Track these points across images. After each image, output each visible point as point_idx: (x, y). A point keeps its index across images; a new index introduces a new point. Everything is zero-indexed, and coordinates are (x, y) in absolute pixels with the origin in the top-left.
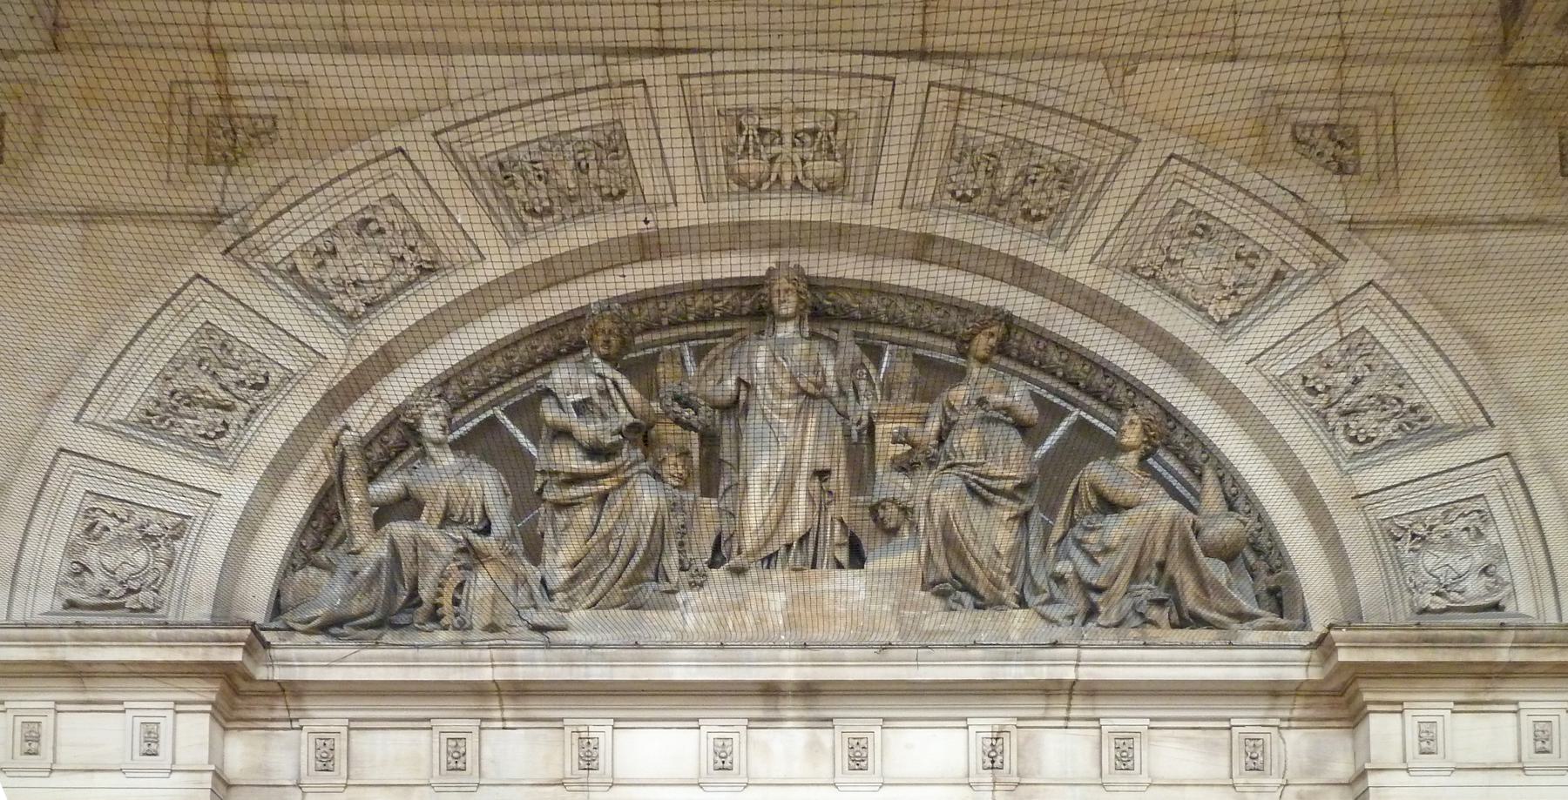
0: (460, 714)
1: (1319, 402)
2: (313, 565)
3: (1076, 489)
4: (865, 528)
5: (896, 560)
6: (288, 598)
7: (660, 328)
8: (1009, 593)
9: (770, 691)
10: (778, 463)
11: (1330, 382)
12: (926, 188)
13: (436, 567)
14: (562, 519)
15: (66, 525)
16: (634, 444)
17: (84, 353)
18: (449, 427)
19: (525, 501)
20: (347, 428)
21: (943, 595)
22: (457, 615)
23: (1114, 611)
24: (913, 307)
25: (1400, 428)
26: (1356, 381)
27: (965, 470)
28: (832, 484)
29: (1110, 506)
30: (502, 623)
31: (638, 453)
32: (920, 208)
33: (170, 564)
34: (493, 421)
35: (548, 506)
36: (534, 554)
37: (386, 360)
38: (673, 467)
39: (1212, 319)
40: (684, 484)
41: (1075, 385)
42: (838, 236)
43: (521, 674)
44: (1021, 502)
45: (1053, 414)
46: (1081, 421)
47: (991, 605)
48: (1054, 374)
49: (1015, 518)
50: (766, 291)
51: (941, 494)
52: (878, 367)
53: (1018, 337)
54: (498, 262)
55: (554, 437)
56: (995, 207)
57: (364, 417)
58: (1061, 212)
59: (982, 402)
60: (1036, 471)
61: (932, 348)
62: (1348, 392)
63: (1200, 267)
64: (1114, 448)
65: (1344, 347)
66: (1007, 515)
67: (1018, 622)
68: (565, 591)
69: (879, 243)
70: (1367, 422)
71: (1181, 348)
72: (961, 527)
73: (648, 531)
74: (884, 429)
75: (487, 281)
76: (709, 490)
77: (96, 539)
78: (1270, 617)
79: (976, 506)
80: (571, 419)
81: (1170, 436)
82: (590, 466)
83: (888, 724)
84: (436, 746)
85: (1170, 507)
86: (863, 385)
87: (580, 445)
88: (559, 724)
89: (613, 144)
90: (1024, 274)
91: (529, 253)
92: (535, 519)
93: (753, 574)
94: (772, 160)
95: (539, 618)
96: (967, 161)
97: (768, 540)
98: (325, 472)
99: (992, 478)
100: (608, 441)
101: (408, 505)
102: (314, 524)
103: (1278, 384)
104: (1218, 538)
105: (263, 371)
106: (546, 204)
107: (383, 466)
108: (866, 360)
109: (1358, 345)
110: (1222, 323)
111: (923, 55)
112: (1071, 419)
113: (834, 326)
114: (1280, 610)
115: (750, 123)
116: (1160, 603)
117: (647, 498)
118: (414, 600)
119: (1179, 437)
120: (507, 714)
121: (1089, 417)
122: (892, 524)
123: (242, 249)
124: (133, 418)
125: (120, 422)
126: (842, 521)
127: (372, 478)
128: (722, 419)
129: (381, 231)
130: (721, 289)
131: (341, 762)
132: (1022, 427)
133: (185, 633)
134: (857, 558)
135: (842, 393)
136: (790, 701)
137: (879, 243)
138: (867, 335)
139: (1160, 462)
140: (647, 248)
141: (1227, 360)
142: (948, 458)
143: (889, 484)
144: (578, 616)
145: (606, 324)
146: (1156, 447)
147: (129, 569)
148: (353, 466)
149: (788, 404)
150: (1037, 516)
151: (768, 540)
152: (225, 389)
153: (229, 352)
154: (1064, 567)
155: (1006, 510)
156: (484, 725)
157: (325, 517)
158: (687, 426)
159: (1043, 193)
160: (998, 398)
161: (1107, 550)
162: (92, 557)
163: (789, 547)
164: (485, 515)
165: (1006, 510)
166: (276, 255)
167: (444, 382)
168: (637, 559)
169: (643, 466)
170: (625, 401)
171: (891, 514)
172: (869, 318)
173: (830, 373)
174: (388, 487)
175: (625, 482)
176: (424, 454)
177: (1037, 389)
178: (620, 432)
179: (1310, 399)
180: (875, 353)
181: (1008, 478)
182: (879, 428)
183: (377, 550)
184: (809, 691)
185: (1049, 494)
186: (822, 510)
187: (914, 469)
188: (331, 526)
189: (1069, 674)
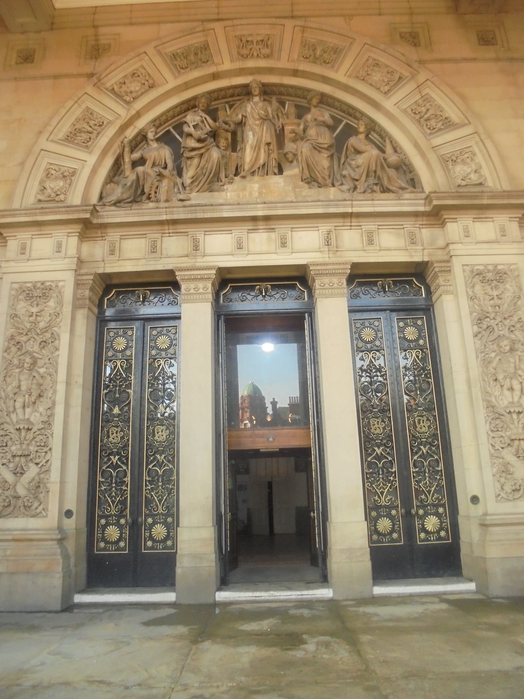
3: (347, 147)
5: (292, 171)
6: (104, 194)
9: (254, 219)
12: (295, 56)
14: (189, 162)
15: (40, 174)
17: (51, 118)
19: (178, 156)
20: (126, 137)
24: (294, 90)
25: (443, 124)
26: (428, 110)
27: (312, 141)
28: (271, 147)
31: (212, 140)
33: (70, 185)
36: (180, 174)
37: (138, 115)
38: (223, 143)
39: (382, 92)
40: (226, 149)
44: (331, 151)
49: (328, 157)
51: (305, 148)
52: (285, 110)
56: (315, 60)
57: (131, 133)
59: (315, 120)
60: (334, 141)
61: (300, 102)
62: (426, 113)
63: (377, 77)
76: (234, 150)
77: (49, 178)
79: (316, 152)
80: (192, 130)
81: (373, 127)
82: (197, 145)
83: (293, 229)
87: (195, 139)
89: (205, 47)
92: (181, 161)
96: (307, 47)
99: (321, 144)
105: (102, 121)
107: (135, 147)
110: (385, 93)
111: (292, 17)
115: (244, 40)
116: (376, 184)
117: (215, 154)
119: (377, 128)
121: (349, 122)
124: (63, 138)
125: (60, 140)
127: (132, 151)
131: (117, 252)
132: (328, 127)
133: (72, 209)
140: (215, 76)
142: (306, 137)
143: (290, 146)
147: (58, 188)
149: (257, 122)
152: (90, 127)
153: (93, 115)
157: (117, 167)
158: (227, 131)
160: (321, 118)
162: (47, 185)
164: (165, 163)
166: (108, 85)
167: (154, 120)
172: (281, 94)
173: (270, 112)
175: (208, 150)
178: (207, 134)
181: (325, 144)
183: (133, 177)
185: (339, 148)
188: (119, 168)
189: (350, 210)
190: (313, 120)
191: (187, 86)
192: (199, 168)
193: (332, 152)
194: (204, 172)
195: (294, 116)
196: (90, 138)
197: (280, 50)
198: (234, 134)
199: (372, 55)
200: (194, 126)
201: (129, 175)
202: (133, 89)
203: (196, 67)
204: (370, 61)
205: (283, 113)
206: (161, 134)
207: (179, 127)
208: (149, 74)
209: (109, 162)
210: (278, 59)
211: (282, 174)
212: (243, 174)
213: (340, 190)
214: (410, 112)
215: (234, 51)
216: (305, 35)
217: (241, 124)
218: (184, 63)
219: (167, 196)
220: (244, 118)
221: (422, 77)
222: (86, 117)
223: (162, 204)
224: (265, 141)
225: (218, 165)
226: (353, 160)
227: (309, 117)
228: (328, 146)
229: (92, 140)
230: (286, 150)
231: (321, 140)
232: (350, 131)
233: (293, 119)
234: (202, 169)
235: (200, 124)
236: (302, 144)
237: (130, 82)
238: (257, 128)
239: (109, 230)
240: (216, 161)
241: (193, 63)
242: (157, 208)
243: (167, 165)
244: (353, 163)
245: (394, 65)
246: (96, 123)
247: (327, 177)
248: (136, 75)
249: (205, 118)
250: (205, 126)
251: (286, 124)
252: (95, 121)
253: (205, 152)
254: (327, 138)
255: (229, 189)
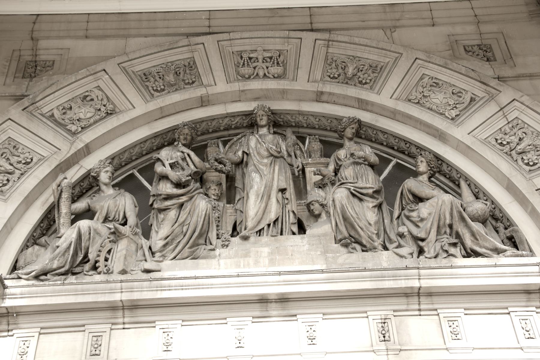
0: (101, 321)
1: (507, 149)
2: (37, 245)
4: (304, 216)
5: (321, 229)
7: (209, 133)
8: (378, 243)
10: (263, 187)
11: (508, 140)
12: (318, 75)
13: (99, 241)
14: (161, 216)
16: (196, 181)
18: (112, 178)
21: (346, 246)
22: (106, 266)
23: (432, 251)
26: (520, 139)
27: (349, 186)
28: (287, 195)
29: (419, 199)
30: (128, 270)
31: (198, 185)
32: (315, 81)
34: (132, 175)
35: (156, 210)
36: (147, 235)
38: (214, 190)
41: (393, 148)
42: (283, 94)
43: (136, 296)
44: (378, 199)
45: (385, 161)
46: (397, 163)
47: (370, 250)
48: (382, 144)
49: (375, 207)
50: (254, 116)
52: (304, 144)
53: (364, 129)
54: (141, 108)
55: (160, 180)
57: (74, 174)
58: (375, 81)
59: (352, 155)
60: (381, 185)
64: (416, 174)
65: (510, 125)
66: (371, 205)
67: (385, 258)
68: (160, 252)
69: (301, 96)
70: (532, 156)
71: (437, 130)
72: (350, 212)
73: (202, 220)
74: (309, 170)
75: (137, 117)
78: (511, 251)
79: (356, 201)
80: (167, 170)
82: (176, 191)
84: (86, 341)
85: (447, 198)
86: (298, 152)
88: (153, 325)
90: (363, 104)
91: (153, 105)
92: (149, 217)
93: (252, 239)
94: (255, 68)
95: (148, 265)
97: (259, 222)
98: (52, 200)
99: (361, 188)
100: (184, 180)
101: (89, 213)
102: (42, 225)
103: (485, 142)
104: (475, 212)
105: (31, 157)
106: (162, 87)
108: (299, 142)
109: (516, 125)
112: (394, 161)
113: (283, 129)
114: (516, 246)
115: (245, 56)
117: (202, 205)
118: (85, 260)
119: (445, 168)
120: (126, 320)
122: (317, 212)
123: (31, 108)
126: (293, 212)
127: (74, 201)
128: (235, 169)
129: (92, 100)
130: (234, 116)
132: (372, 166)
134: (302, 229)
135: (289, 155)
136: (273, 305)
137: (301, 96)
138: (298, 132)
139: (437, 179)
141: (458, 133)
142: (339, 181)
143: (315, 195)
144: (167, 263)
145: (186, 131)
146: (435, 172)
148: (65, 195)
149: (265, 161)
150: (385, 207)
151: (259, 222)
152: (11, 164)
153: (17, 150)
154: (403, 229)
155: (370, 203)
156: (114, 327)
158: (221, 171)
159: (369, 75)
161: (422, 220)
163: (269, 225)
165: (370, 203)
167: (112, 158)
168: (196, 234)
169: (201, 190)
170: (193, 162)
171: (316, 208)
174: (81, 205)
175: (191, 198)
176: (100, 190)
177: (378, 152)
179: (501, 148)
180: (302, 139)
181: (370, 188)
182: (307, 170)
184: (284, 300)
186: (284, 207)
187: (324, 187)
190: (348, 156)
191: (162, 113)
192: (177, 224)
193: (380, 200)
194: (185, 230)
195: (319, 153)
196: (8, 180)
197: (297, 68)
198: (230, 179)
199: (427, 72)
200: (172, 166)
201: (68, 234)
202: (82, 116)
203: (176, 90)
204: (426, 79)
205: (303, 150)
206: (120, 179)
207: (148, 171)
208: (108, 97)
209: (35, 214)
210: (293, 80)
211: (305, 233)
212: (244, 233)
213: (397, 254)
214: (494, 142)
215: (232, 71)
216: (330, 50)
217: (240, 164)
218: (160, 84)
219: (125, 265)
220: (245, 156)
221: (504, 98)
222: (5, 150)
223: (116, 277)
224: (278, 187)
225: (207, 218)
226: (413, 211)
227: (342, 153)
228: (374, 192)
229: (10, 184)
230: (310, 199)
231: (360, 184)
232: (404, 172)
233: (317, 158)
234: (182, 224)
235: (180, 162)
236: (332, 190)
237: (79, 107)
238: (264, 168)
239: (21, 319)
240: (204, 213)
241: (172, 85)
242: (108, 282)
243: (127, 220)
244: (414, 214)
245: (462, 83)
246: (20, 159)
247: (374, 237)
248: (88, 98)
249: (189, 155)
250: (188, 164)
251: (307, 164)
252: (19, 156)
253: (187, 201)
254: (371, 181)
255: (223, 255)
